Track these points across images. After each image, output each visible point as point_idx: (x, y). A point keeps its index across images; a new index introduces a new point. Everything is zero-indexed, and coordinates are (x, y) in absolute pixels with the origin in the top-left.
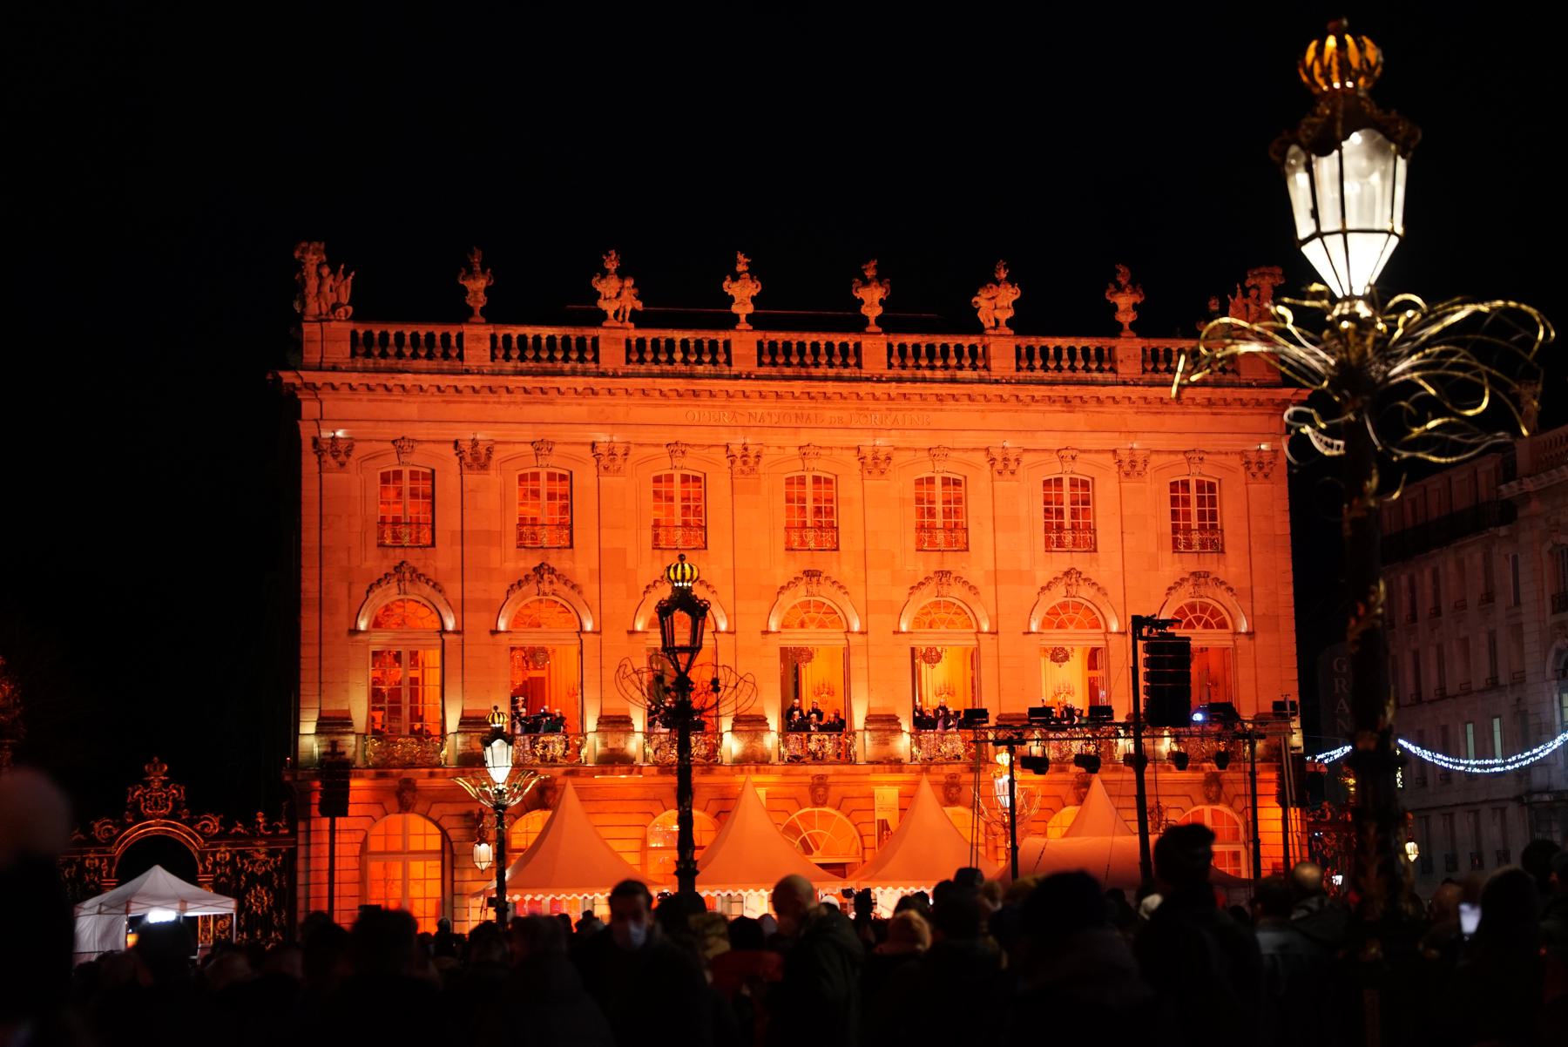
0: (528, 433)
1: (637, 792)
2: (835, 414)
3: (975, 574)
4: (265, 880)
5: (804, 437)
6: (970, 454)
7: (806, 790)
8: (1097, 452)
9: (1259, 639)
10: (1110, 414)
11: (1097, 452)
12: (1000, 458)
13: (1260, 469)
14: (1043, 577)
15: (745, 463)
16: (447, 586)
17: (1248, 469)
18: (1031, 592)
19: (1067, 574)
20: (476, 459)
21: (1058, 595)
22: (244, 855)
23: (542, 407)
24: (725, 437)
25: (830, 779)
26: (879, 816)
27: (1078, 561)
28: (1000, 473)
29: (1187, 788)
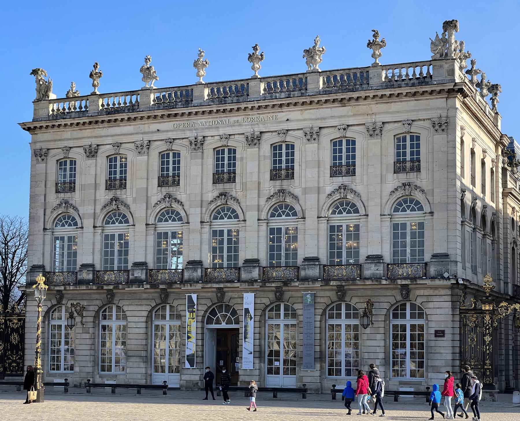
0: (110, 140)
1: (145, 296)
2: (236, 119)
3: (297, 191)
4: (17, 330)
5: (222, 131)
6: (296, 132)
7: (215, 294)
8: (357, 125)
9: (435, 215)
10: (363, 107)
11: (357, 125)
12: (308, 133)
13: (440, 126)
14: (329, 189)
15: (196, 145)
16: (80, 209)
17: (434, 127)
18: (323, 197)
19: (340, 188)
20: (90, 153)
21: (337, 196)
22: (10, 321)
23: (116, 128)
24: (188, 134)
25: (225, 290)
26: (245, 306)
27: (346, 180)
28: (308, 140)
29: (394, 292)
